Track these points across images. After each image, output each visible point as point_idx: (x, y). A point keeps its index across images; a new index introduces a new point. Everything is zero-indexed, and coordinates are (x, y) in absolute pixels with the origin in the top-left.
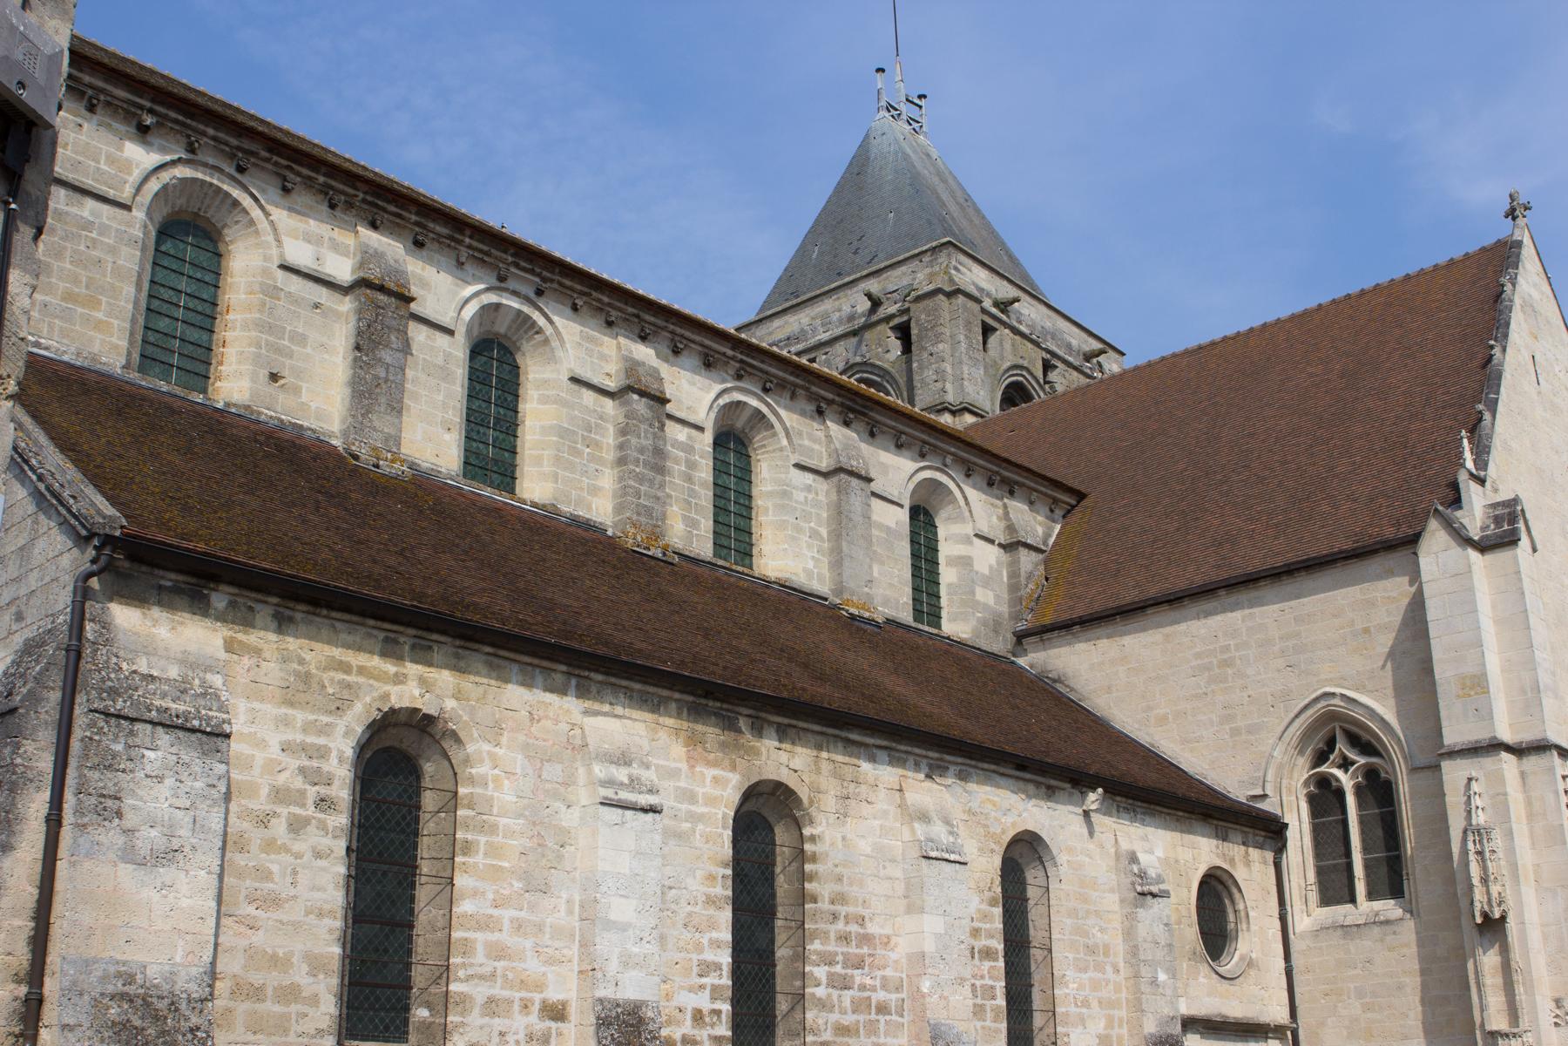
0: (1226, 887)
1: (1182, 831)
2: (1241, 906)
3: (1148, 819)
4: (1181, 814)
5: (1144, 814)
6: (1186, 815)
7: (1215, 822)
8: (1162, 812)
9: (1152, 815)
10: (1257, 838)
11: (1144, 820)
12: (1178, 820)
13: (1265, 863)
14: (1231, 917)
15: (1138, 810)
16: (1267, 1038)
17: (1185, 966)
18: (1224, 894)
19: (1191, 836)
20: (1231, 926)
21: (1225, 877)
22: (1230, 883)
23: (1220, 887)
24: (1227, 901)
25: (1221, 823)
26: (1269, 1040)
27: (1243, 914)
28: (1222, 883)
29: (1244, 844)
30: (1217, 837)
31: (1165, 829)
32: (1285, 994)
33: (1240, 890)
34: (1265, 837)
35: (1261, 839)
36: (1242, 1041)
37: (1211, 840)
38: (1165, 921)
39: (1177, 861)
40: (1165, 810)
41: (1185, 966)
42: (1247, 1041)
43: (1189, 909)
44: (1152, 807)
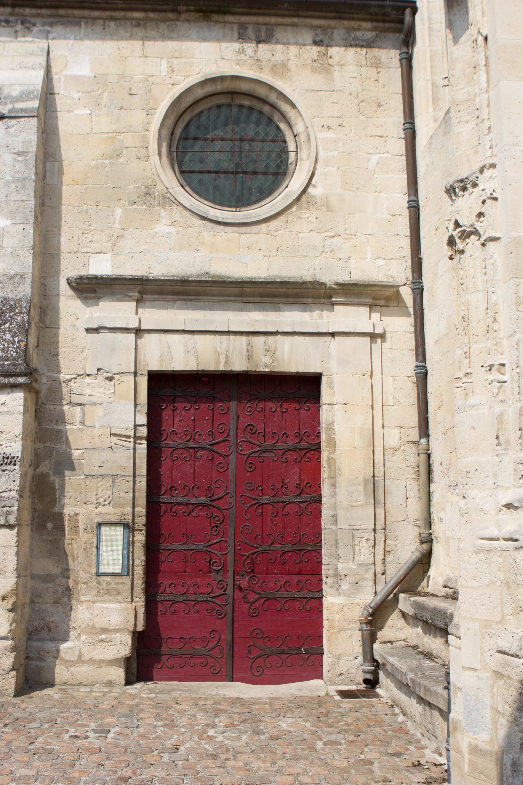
0: (273, 106)
1: (144, 39)
2: (299, 128)
3: (59, 29)
4: (137, 15)
5: (51, 25)
6: (151, 15)
7: (231, 18)
8: (95, 19)
9: (75, 22)
10: (359, 34)
11: (48, 32)
12: (139, 25)
13: (377, 65)
14: (291, 146)
15: (37, 21)
16: (333, 304)
17: (119, 211)
18: (276, 118)
19: (172, 45)
20: (292, 157)
21: (261, 92)
22: (273, 98)
23: (266, 109)
24: (283, 126)
25: (244, 19)
26: (336, 307)
27: (302, 138)
28: (264, 101)
29: (316, 43)
30: (242, 37)
31: (102, 39)
32: (406, 243)
33: (294, 106)
34: (375, 29)
35: (370, 35)
36: (259, 310)
37: (224, 45)
38: (20, 148)
39: (122, 76)
40: (96, 13)
41: (119, 211)
42: (278, 310)
43: (145, 137)
44: (62, 12)
